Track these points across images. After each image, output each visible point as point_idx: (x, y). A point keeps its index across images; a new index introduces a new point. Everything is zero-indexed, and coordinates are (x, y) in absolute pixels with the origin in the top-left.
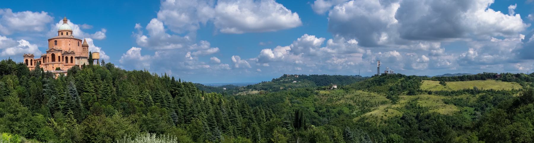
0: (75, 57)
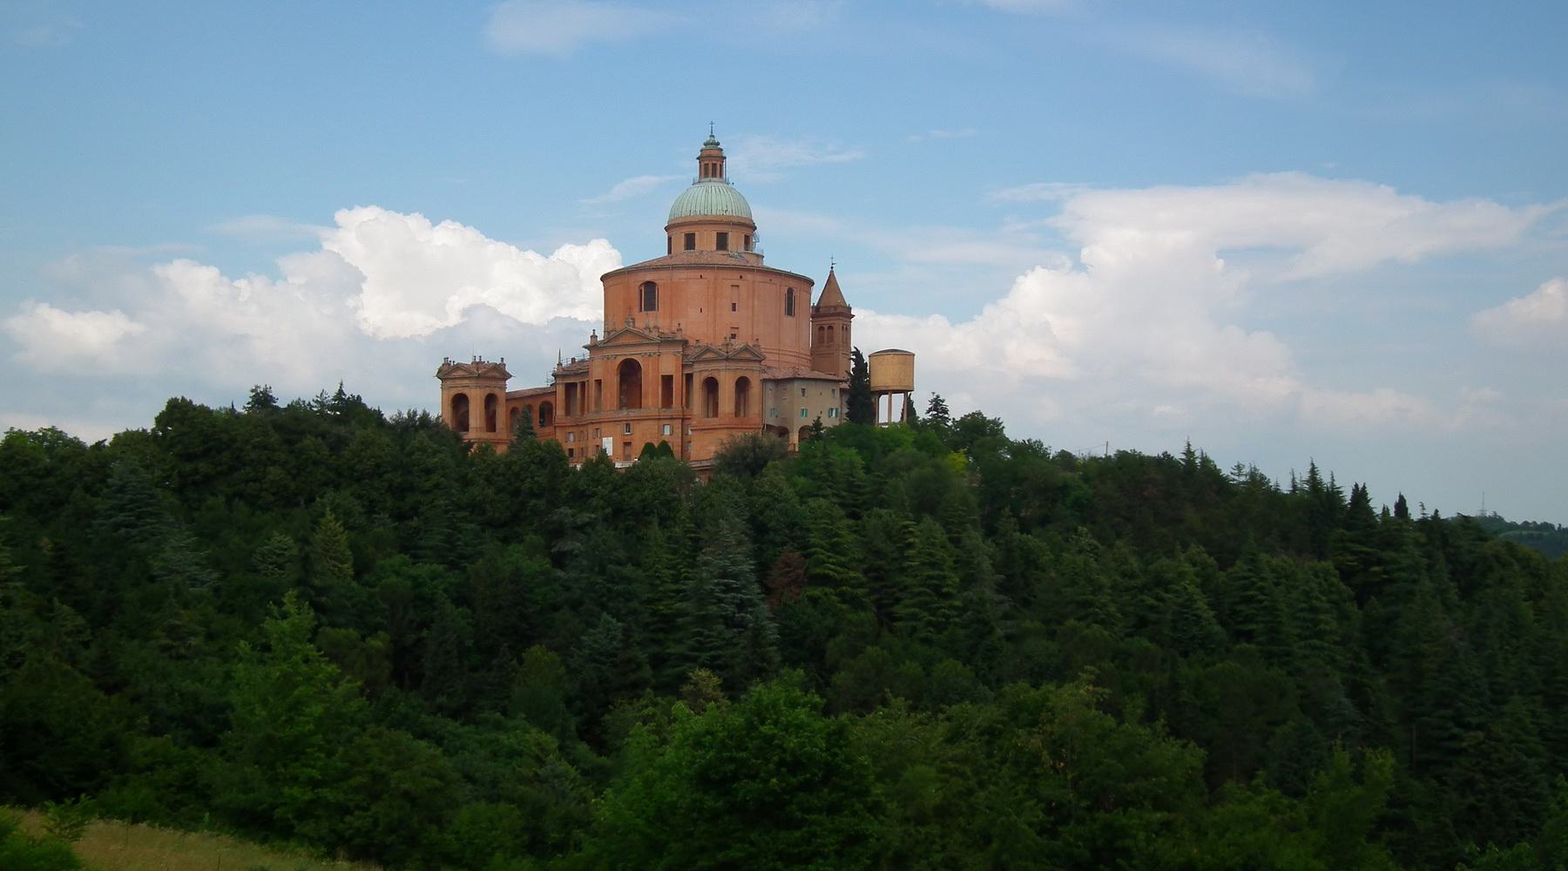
0: (764, 381)
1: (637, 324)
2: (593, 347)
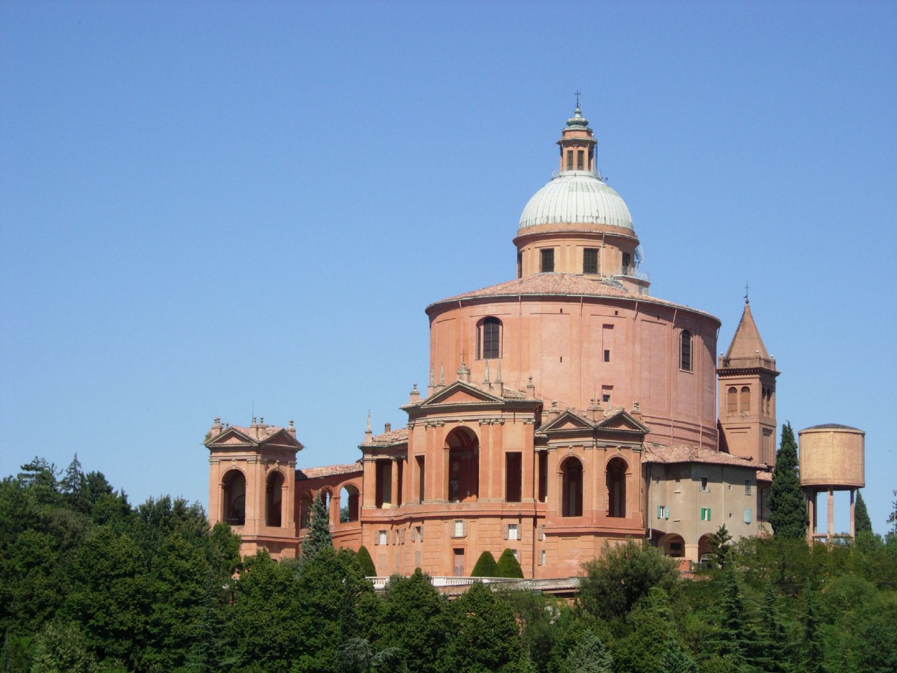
1: (473, 375)
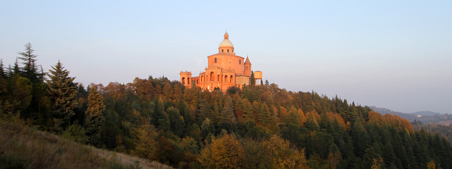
1: (214, 65)
2: (206, 69)
